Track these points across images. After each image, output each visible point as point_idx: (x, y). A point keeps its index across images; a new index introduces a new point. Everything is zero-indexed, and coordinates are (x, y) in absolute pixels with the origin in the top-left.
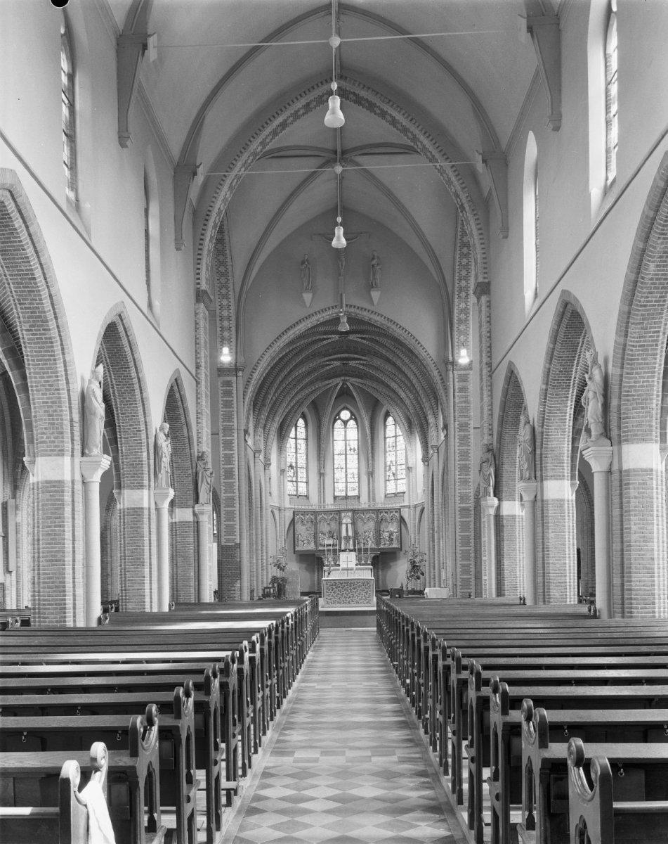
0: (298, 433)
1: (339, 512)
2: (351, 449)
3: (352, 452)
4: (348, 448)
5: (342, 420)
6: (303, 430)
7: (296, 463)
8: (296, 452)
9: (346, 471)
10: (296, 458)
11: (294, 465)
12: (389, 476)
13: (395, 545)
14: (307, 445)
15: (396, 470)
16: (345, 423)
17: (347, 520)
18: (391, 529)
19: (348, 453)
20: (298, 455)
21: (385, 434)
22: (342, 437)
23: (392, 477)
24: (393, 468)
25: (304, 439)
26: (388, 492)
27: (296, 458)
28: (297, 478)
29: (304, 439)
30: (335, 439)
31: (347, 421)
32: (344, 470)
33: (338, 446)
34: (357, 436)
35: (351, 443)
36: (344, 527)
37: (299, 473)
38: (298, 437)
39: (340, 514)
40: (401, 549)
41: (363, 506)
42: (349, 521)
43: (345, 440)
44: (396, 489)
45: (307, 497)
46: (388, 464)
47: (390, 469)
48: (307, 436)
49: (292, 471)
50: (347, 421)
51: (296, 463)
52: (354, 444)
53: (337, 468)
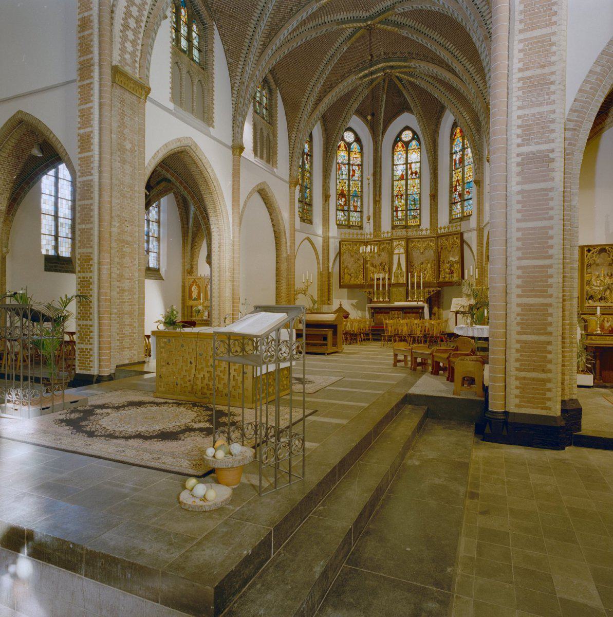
0: (351, 158)
1: (392, 240)
2: (412, 173)
3: (414, 176)
4: (409, 172)
5: (404, 142)
6: (358, 156)
7: (349, 191)
8: (349, 180)
9: (406, 200)
10: (349, 185)
11: (346, 193)
12: (455, 198)
13: (456, 278)
14: (362, 172)
15: (463, 189)
16: (407, 144)
17: (399, 251)
18: (451, 259)
19: (409, 177)
20: (351, 182)
21: (451, 148)
22: (402, 161)
23: (458, 199)
24: (459, 188)
25: (358, 165)
26: (454, 217)
27: (349, 185)
28: (349, 206)
29: (358, 165)
30: (395, 163)
31: (410, 141)
32: (404, 197)
33: (400, 170)
34: (419, 157)
35: (413, 165)
36: (395, 258)
37: (352, 202)
38: (351, 162)
39: (392, 243)
40: (459, 284)
41: (424, 232)
42: (402, 251)
43: (407, 163)
44: (463, 212)
45: (361, 227)
46: (454, 183)
47: (456, 189)
48: (362, 161)
49: (343, 199)
50: (410, 141)
51: (349, 191)
52: (415, 167)
53: (397, 196)
